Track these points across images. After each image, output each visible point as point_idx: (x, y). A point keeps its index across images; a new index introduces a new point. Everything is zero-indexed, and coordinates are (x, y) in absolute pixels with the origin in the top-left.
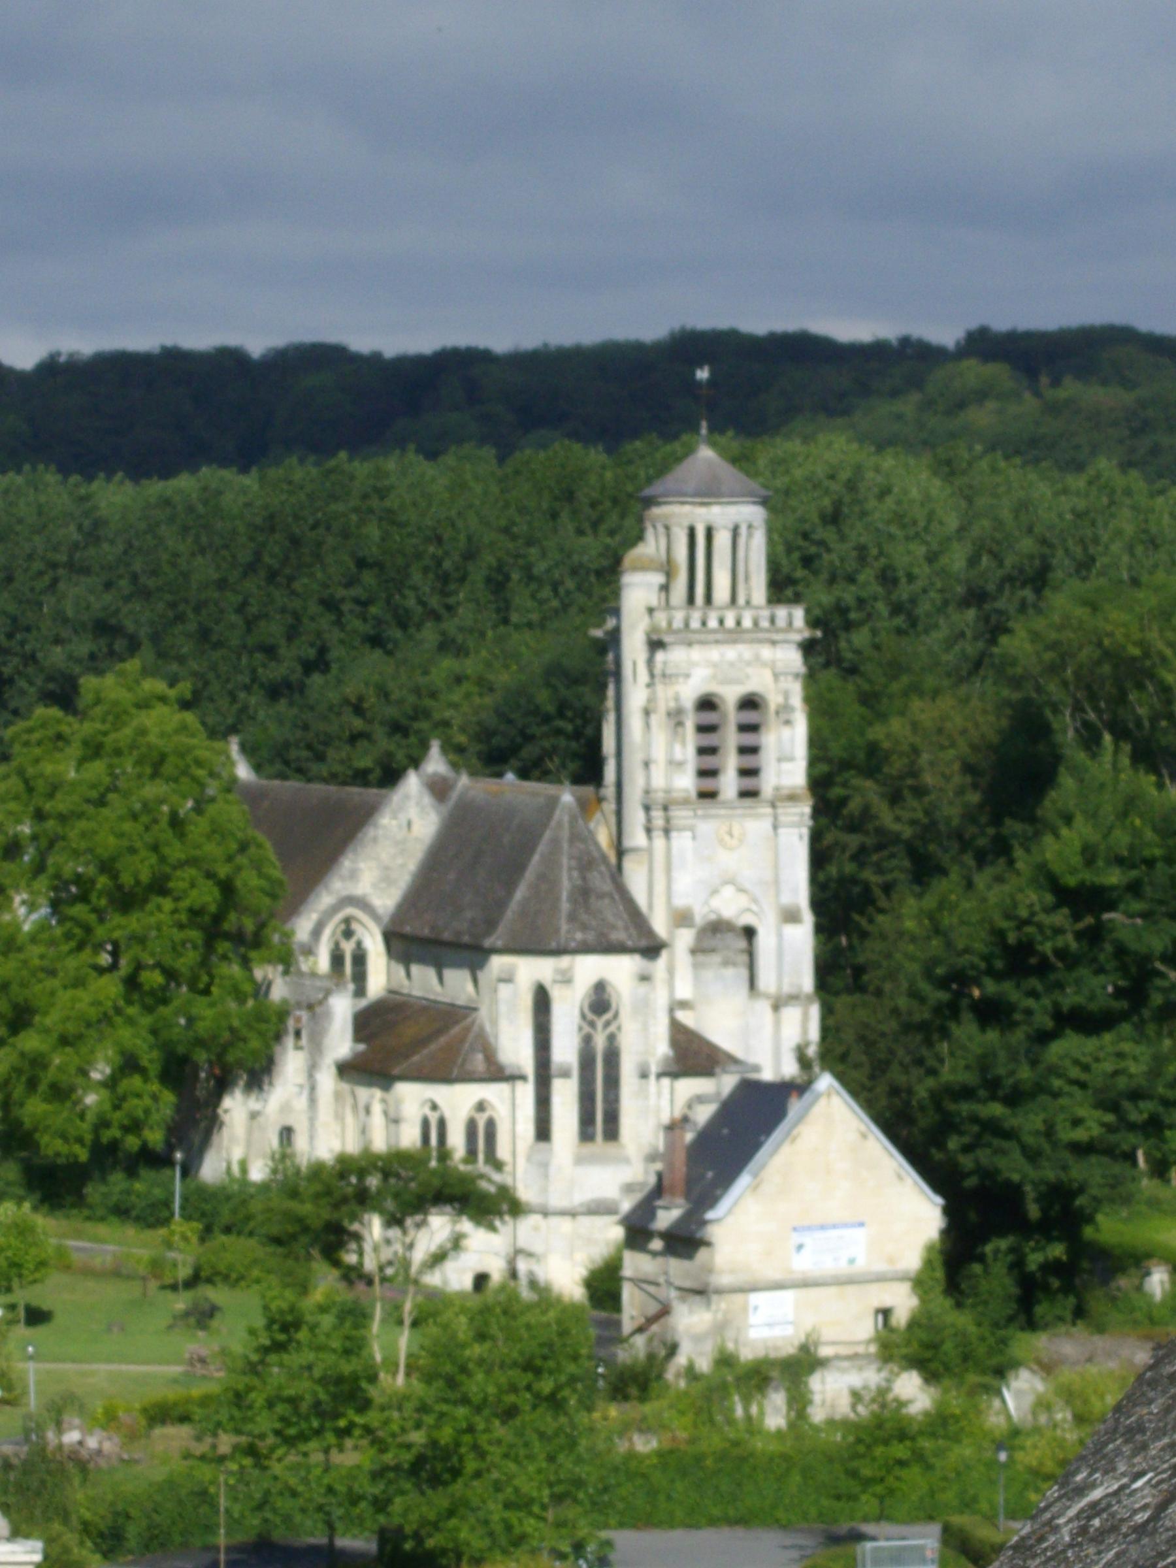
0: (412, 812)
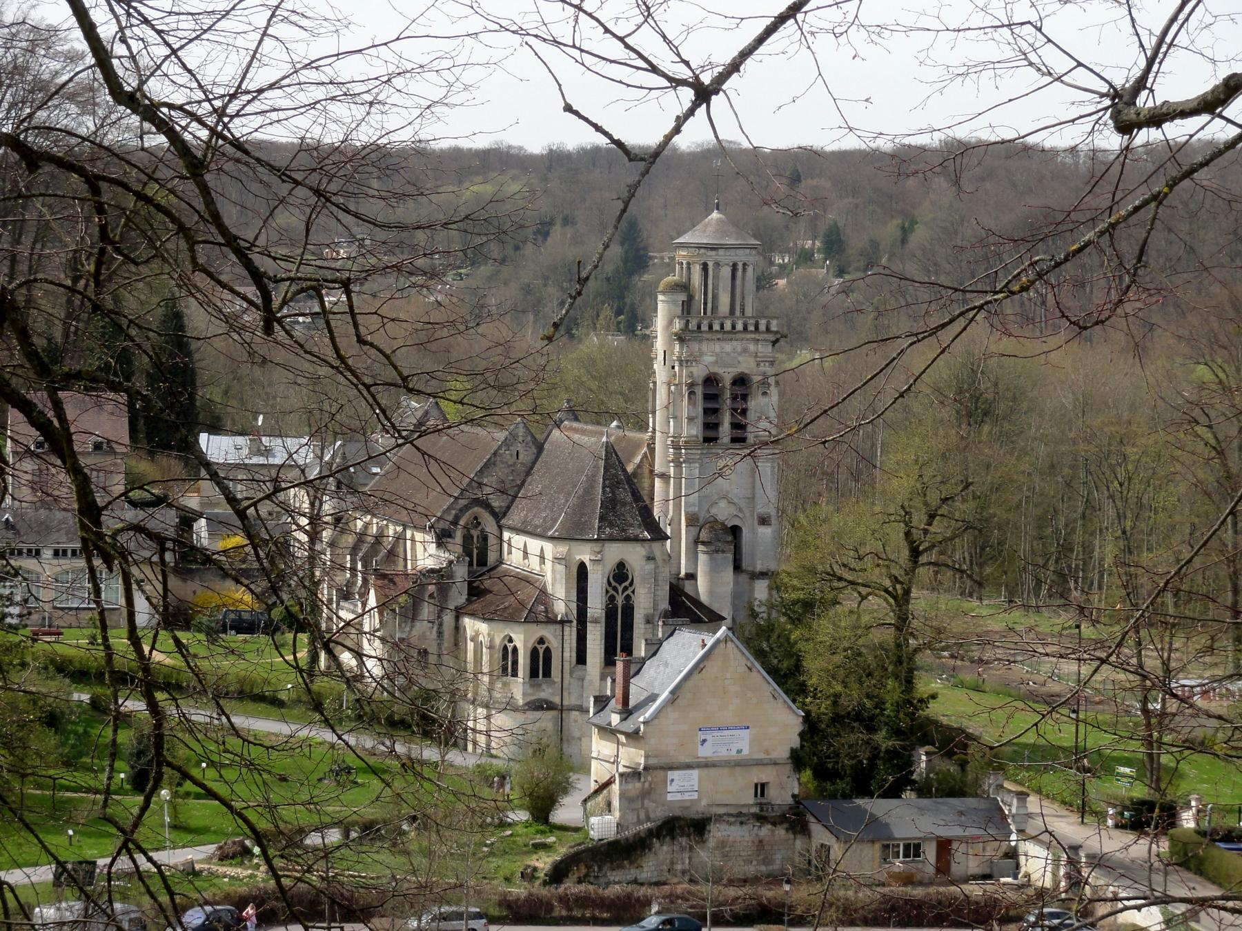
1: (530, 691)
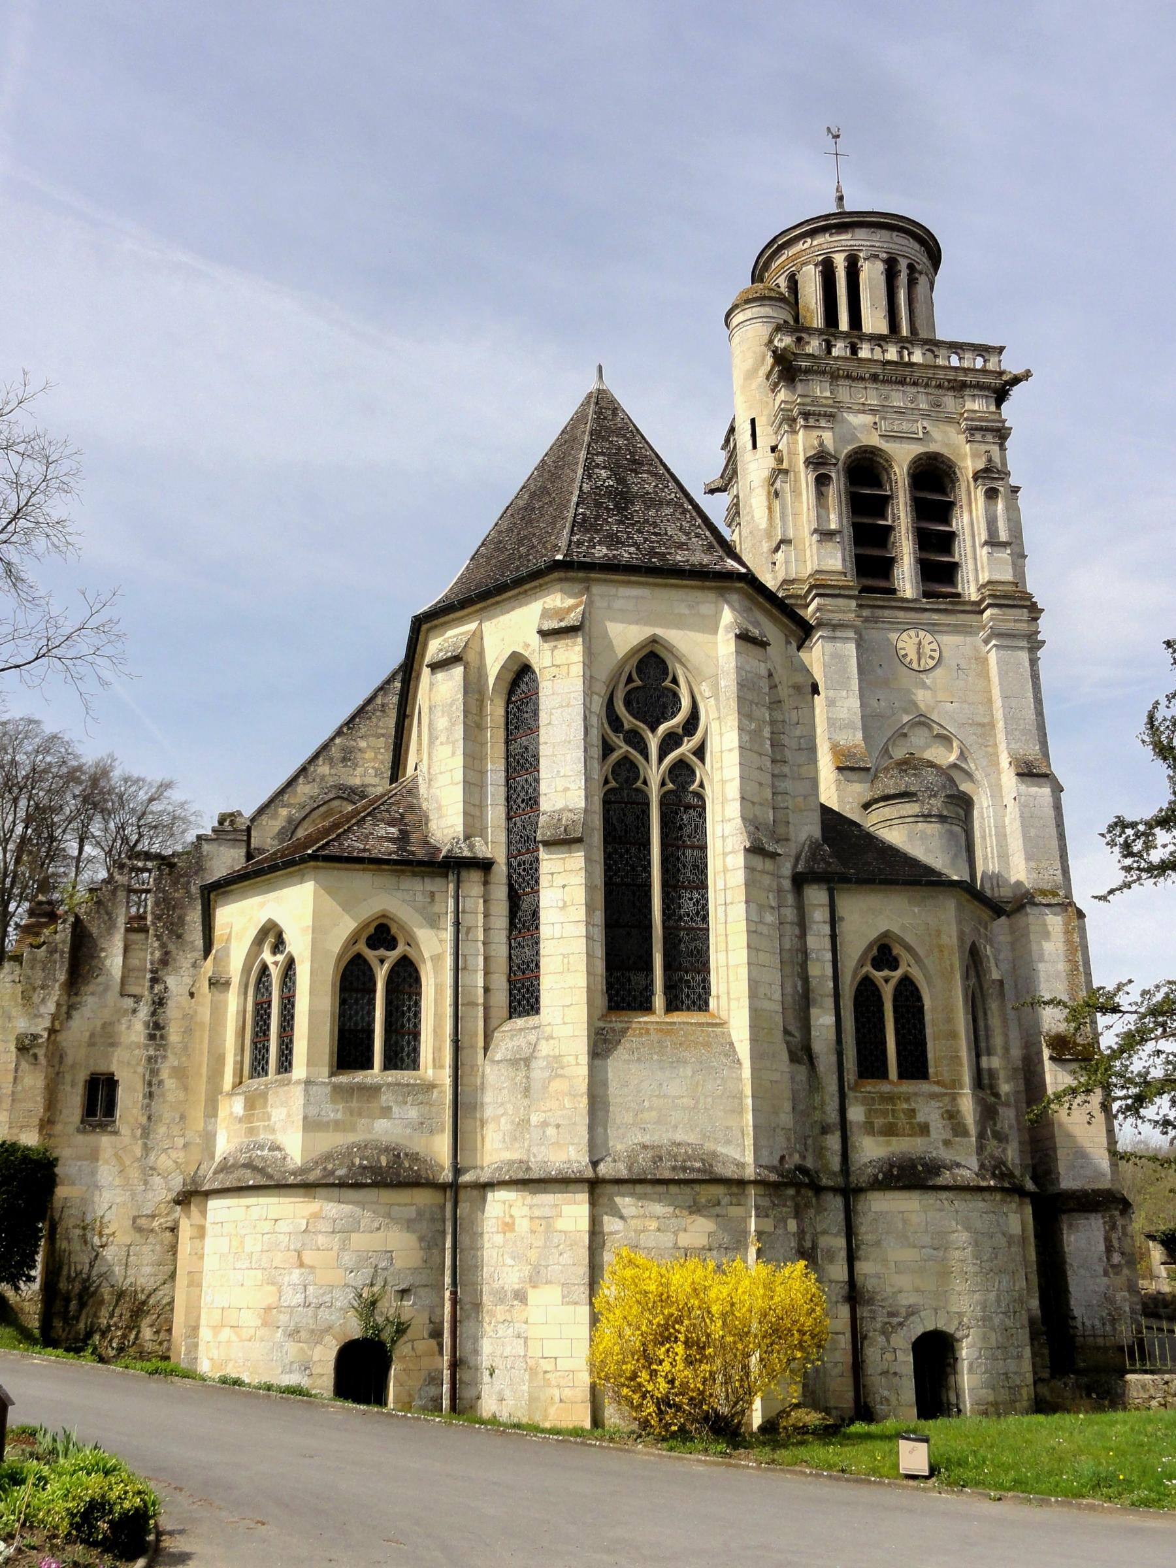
1: (333, 1112)
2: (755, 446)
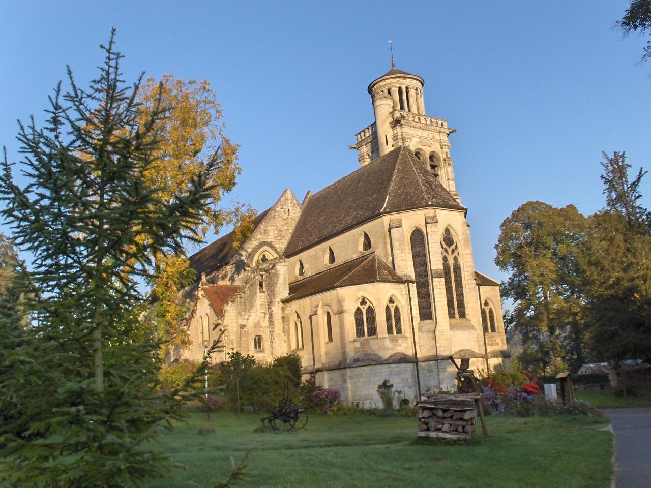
0: (290, 206)
2: (387, 144)
